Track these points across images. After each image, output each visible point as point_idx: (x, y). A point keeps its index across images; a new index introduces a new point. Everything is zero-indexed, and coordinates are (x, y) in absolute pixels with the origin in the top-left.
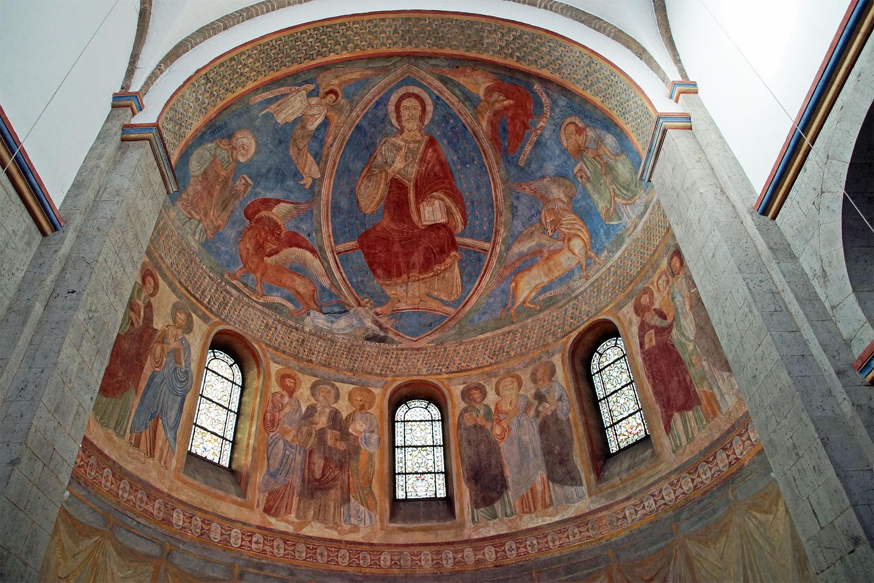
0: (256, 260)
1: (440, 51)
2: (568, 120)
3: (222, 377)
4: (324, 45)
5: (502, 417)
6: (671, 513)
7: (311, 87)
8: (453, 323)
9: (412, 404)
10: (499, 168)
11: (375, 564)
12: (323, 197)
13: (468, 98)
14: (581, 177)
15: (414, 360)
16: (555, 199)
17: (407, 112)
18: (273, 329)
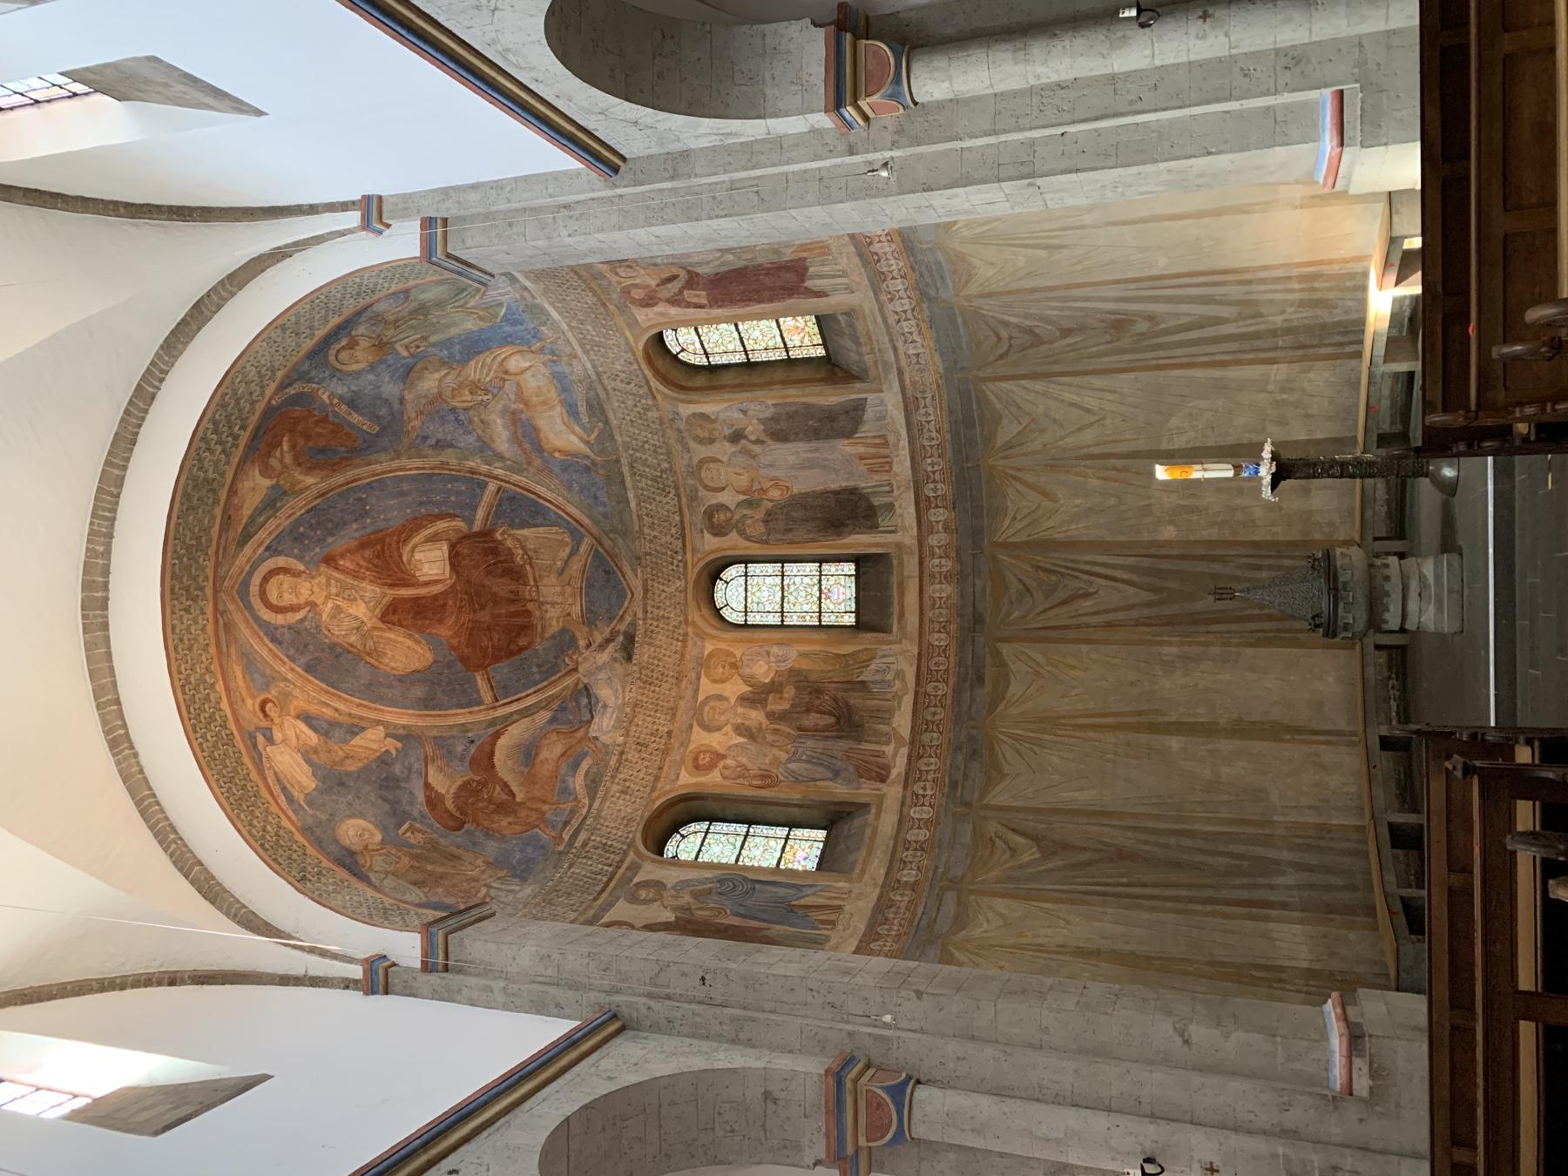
0: (523, 813)
1: (214, 543)
2: (332, 359)
3: (702, 845)
4: (212, 716)
5: (756, 486)
6: (925, 306)
7: (260, 739)
8: (607, 543)
9: (719, 602)
10: (376, 462)
11: (944, 651)
12: (413, 721)
13: (271, 504)
14: (418, 347)
15: (663, 597)
16: (439, 386)
17: (286, 596)
18: (627, 784)
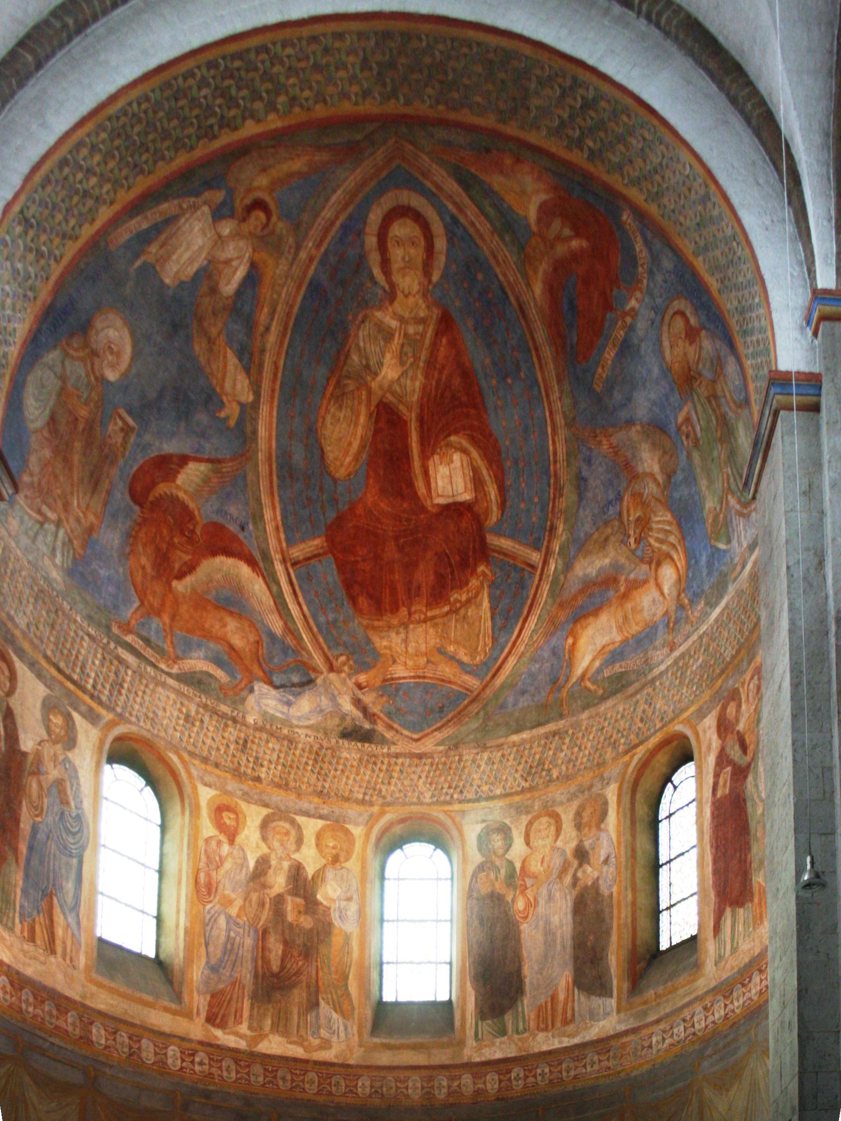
0: (158, 588)
